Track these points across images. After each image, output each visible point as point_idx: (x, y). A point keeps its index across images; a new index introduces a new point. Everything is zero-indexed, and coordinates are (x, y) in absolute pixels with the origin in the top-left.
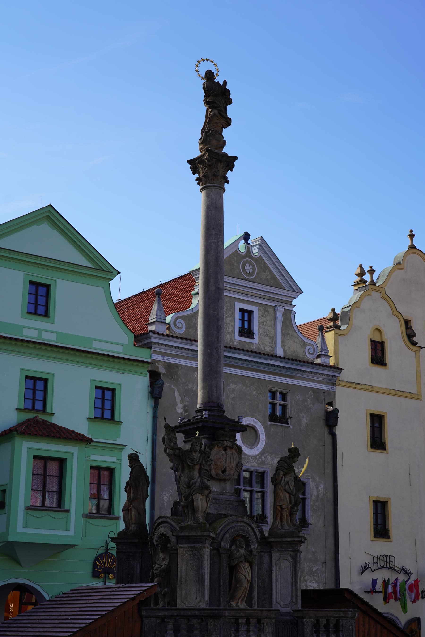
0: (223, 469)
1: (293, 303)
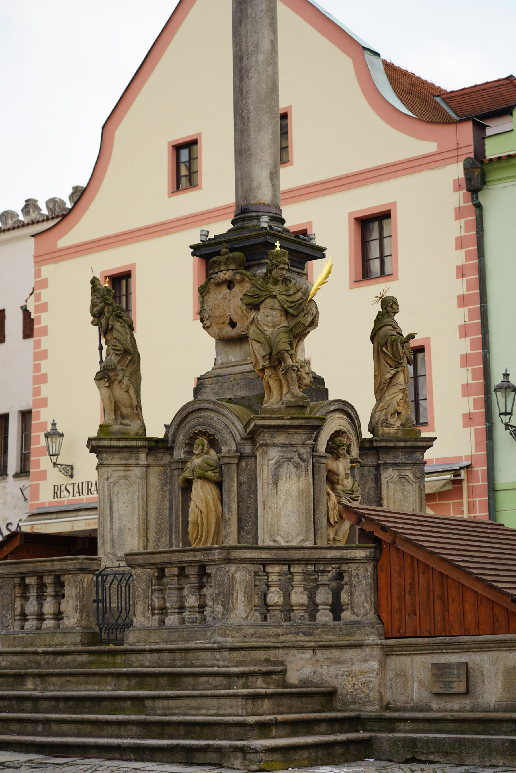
0: (228, 321)
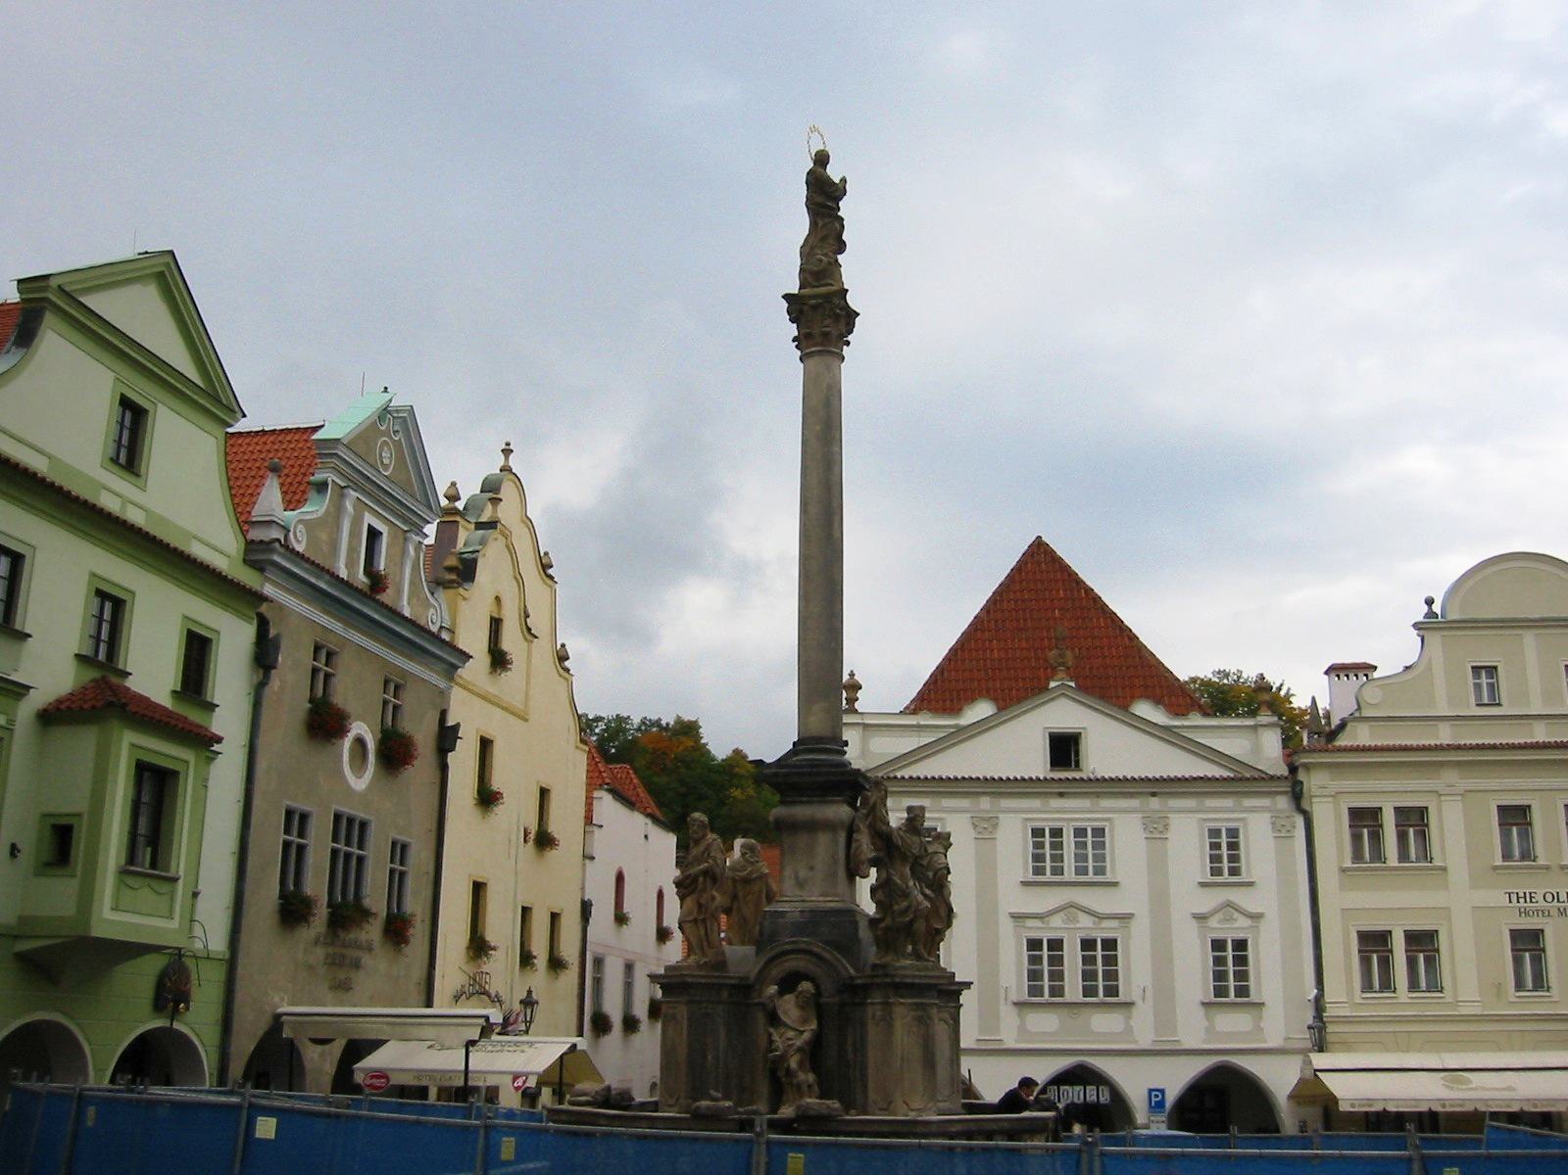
1: (425, 530)
